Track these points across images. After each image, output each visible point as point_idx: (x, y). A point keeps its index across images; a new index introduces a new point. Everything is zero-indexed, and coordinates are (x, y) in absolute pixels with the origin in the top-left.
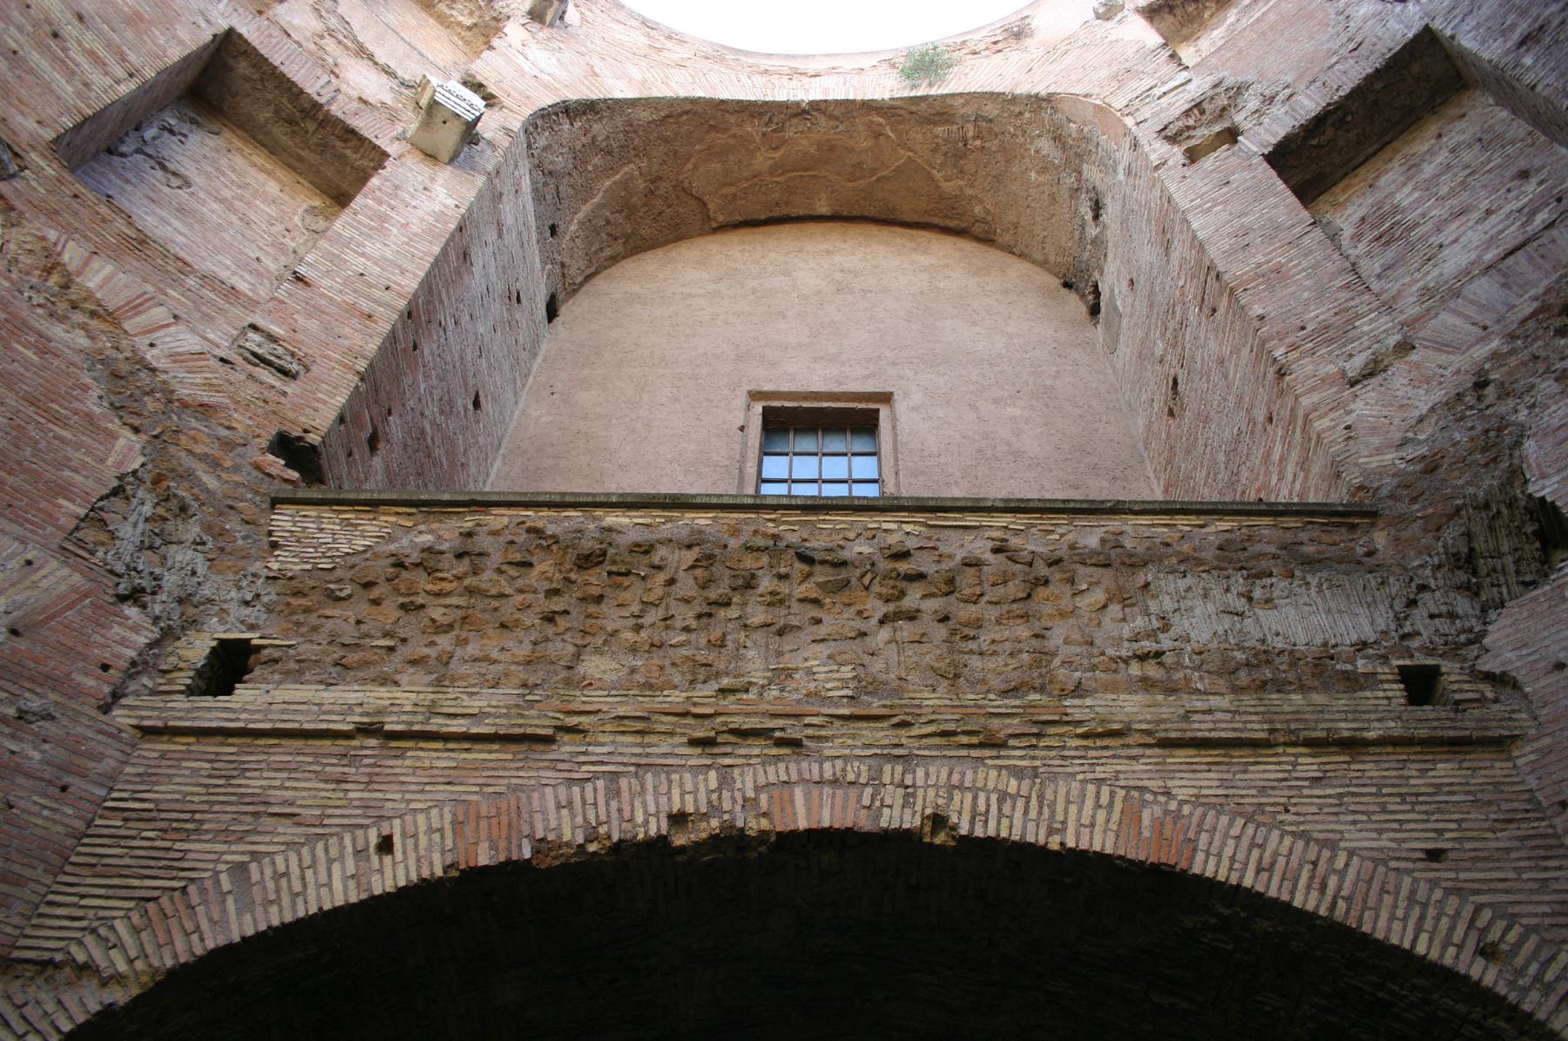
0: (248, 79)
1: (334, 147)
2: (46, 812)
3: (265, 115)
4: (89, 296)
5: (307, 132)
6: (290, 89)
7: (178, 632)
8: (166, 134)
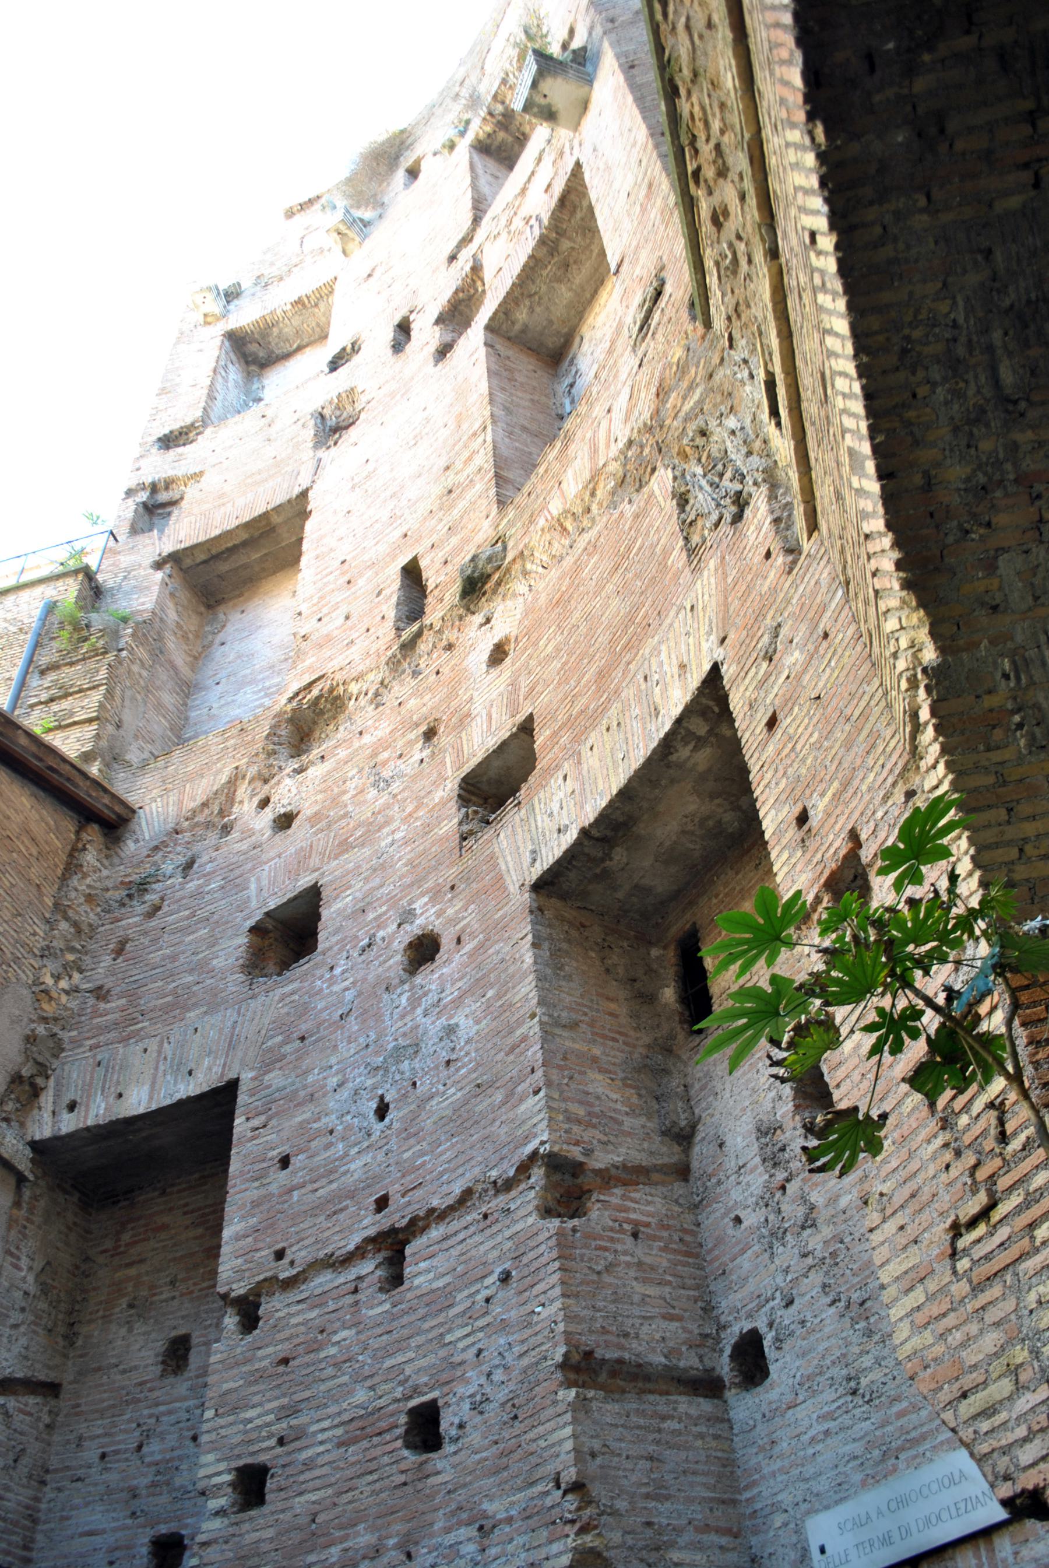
0: (532, 310)
1: (582, 219)
2: (833, 664)
3: (564, 294)
4: (580, 496)
5: (573, 248)
6: (532, 269)
7: (770, 463)
8: (573, 391)
